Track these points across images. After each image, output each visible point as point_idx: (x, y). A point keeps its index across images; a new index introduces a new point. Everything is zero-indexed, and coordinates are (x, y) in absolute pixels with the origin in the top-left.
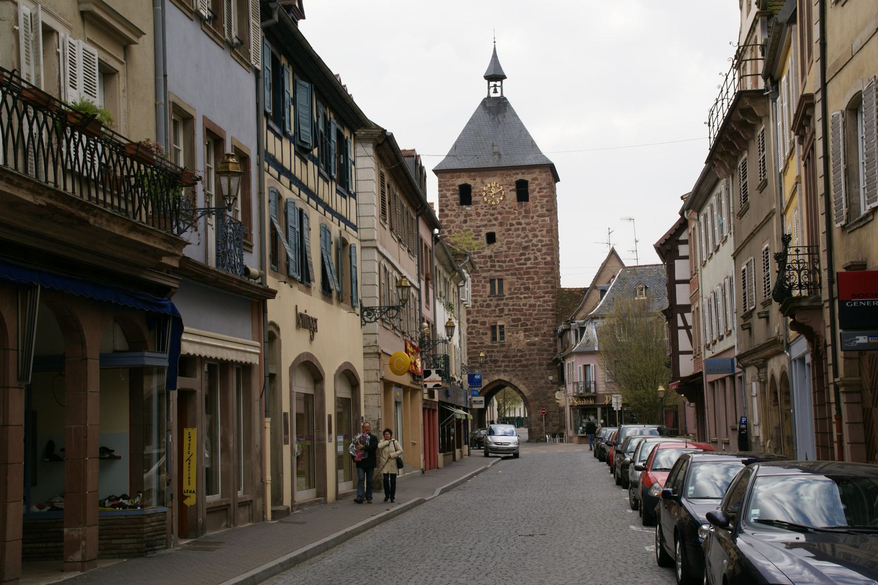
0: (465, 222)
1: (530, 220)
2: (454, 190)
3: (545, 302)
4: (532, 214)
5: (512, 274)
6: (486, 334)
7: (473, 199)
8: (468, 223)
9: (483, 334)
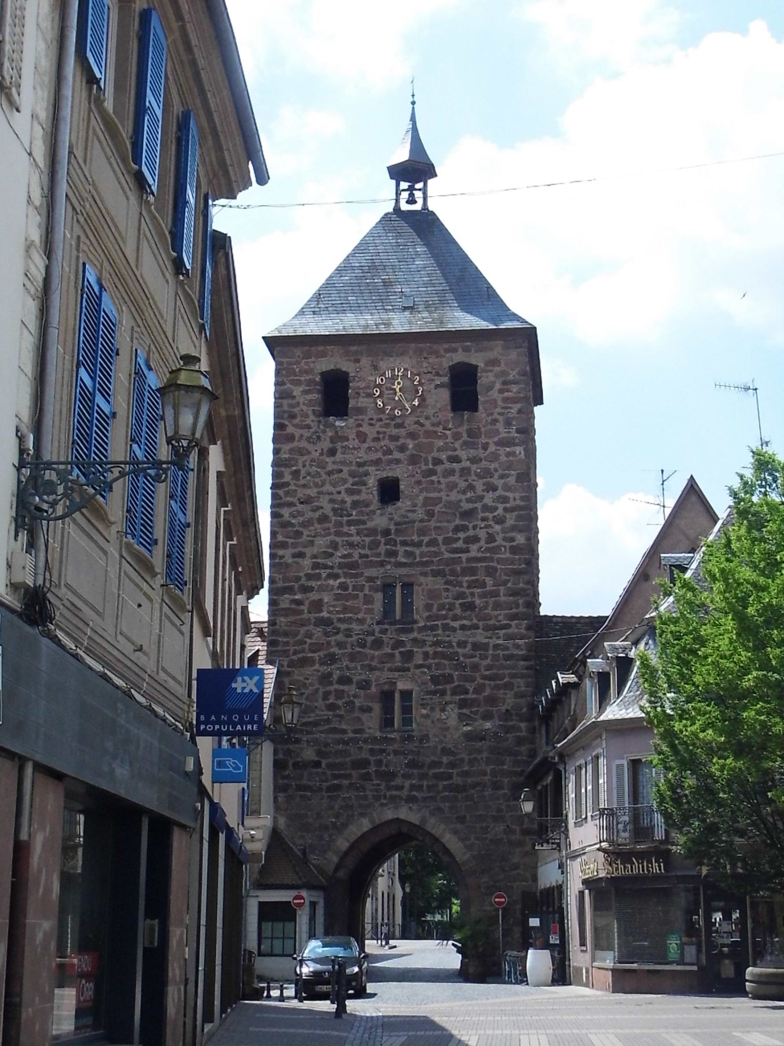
0: (332, 452)
1: (481, 453)
2: (310, 382)
3: (508, 637)
4: (483, 440)
5: (436, 574)
6: (370, 710)
8: (339, 456)
9: (363, 710)
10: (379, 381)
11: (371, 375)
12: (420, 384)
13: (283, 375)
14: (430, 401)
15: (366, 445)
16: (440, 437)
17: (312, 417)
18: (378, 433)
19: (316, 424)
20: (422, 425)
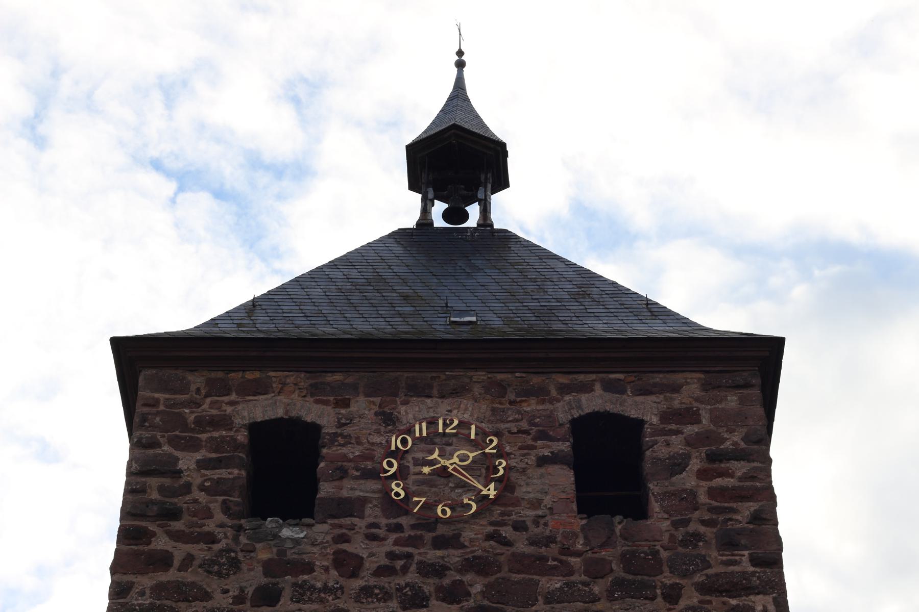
2: (216, 446)
4: (667, 578)
7: (326, 489)
10: (395, 442)
11: (378, 432)
12: (501, 454)
13: (153, 427)
14: (526, 490)
15: (357, 583)
16: (551, 572)
17: (219, 517)
18: (391, 555)
19: (230, 532)
20: (507, 543)
